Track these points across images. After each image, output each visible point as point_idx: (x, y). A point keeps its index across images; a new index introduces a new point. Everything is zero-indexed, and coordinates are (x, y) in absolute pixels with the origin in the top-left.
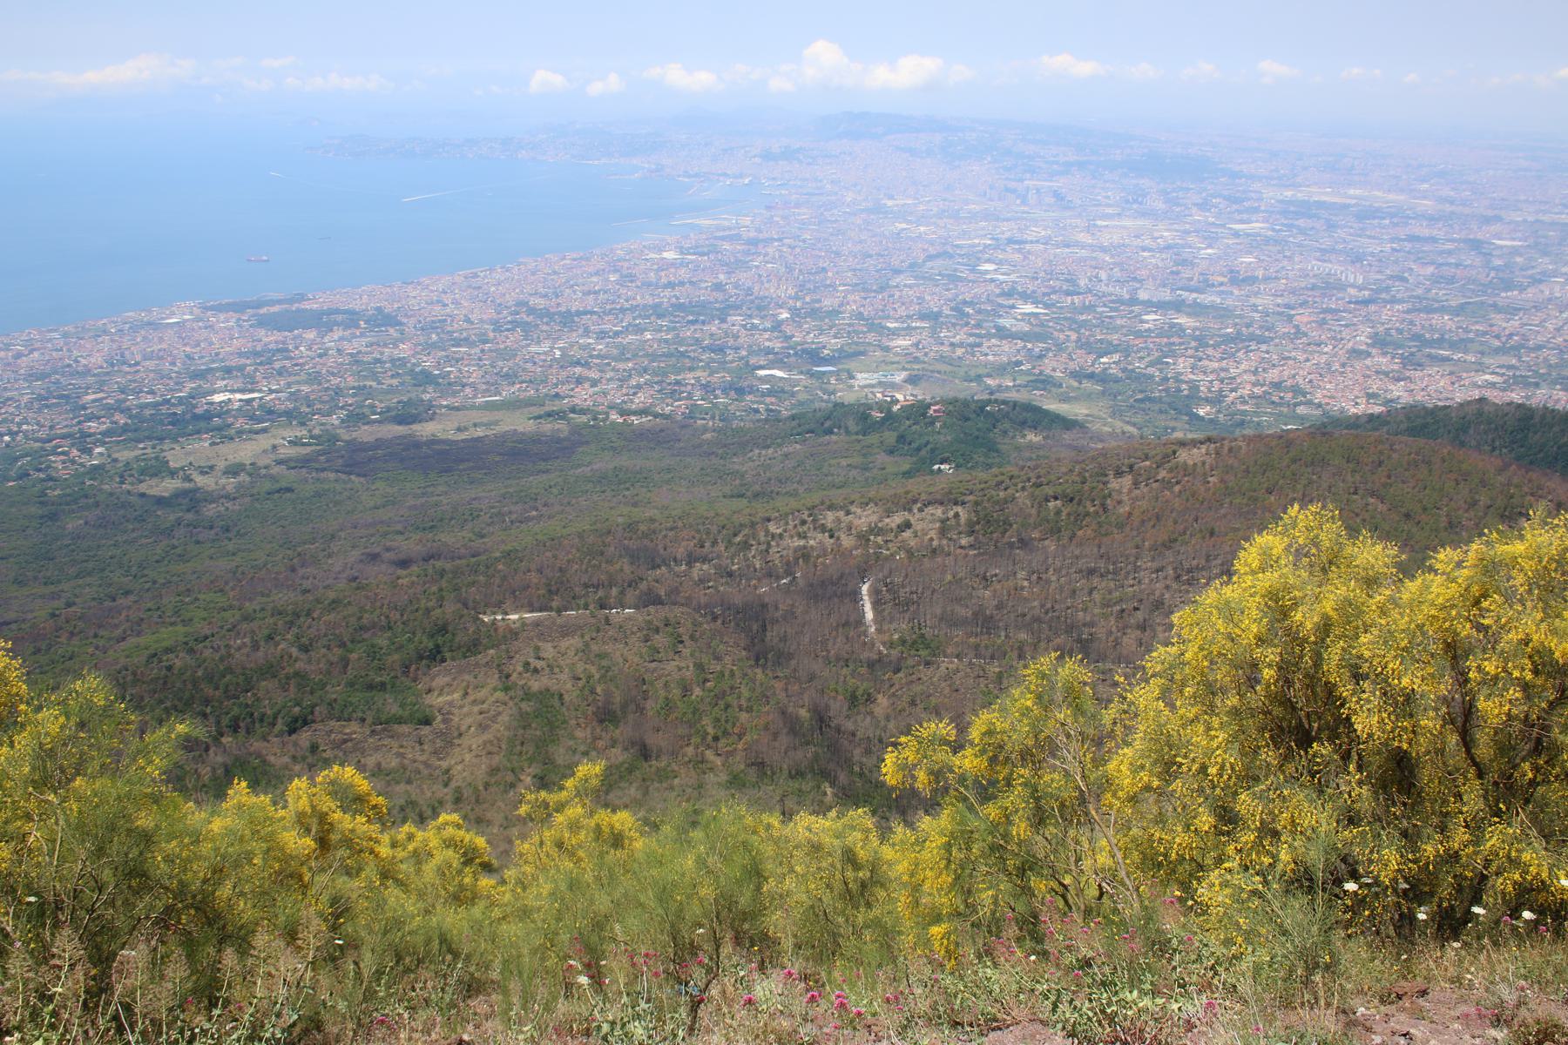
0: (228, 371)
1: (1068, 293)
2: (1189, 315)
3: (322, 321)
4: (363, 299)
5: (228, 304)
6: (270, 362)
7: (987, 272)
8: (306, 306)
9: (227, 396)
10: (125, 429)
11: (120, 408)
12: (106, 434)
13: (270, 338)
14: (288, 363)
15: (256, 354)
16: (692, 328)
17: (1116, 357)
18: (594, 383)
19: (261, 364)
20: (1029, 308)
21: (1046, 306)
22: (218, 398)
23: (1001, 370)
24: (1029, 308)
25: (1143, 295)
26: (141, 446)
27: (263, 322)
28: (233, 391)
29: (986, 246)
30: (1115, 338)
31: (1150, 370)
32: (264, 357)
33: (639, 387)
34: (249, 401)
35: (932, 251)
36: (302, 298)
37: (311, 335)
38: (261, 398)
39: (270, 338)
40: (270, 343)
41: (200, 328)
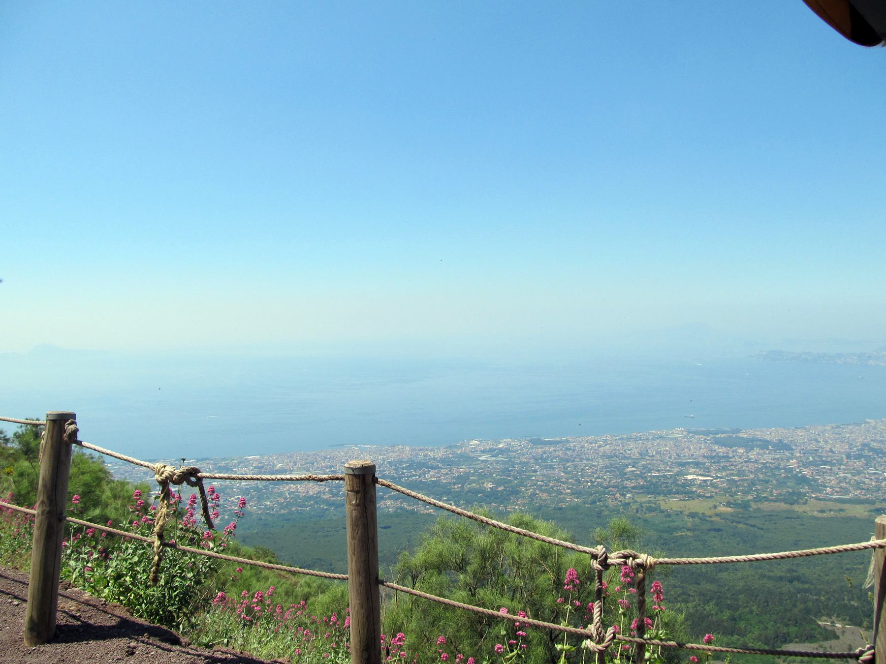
0: (697, 464)
3: (749, 444)
4: (771, 434)
5: (700, 431)
6: (719, 462)
8: (740, 435)
9: (695, 477)
10: (642, 487)
11: (641, 476)
12: (633, 488)
13: (721, 450)
14: (727, 464)
15: (713, 458)
19: (714, 462)
22: (690, 477)
26: (649, 496)
27: (717, 442)
28: (697, 475)
32: (716, 459)
34: (705, 481)
36: (738, 431)
37: (741, 451)
38: (712, 480)
39: (721, 450)
40: (720, 452)
41: (686, 442)
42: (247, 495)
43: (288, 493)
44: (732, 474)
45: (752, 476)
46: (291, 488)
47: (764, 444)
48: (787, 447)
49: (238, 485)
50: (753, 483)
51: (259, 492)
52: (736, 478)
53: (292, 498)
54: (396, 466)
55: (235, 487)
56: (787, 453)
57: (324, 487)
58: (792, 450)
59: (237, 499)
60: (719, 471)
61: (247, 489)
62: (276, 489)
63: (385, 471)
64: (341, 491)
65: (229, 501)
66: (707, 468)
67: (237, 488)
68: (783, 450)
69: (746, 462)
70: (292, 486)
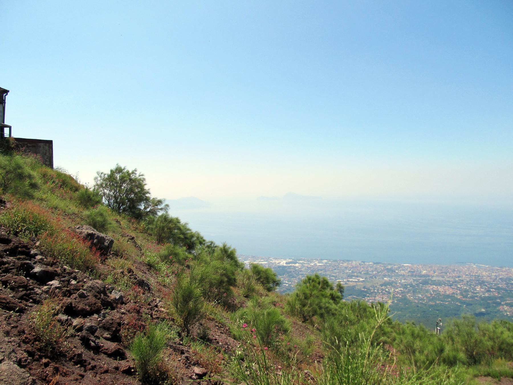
42: (406, 288)
43: (432, 291)
46: (434, 287)
49: (400, 281)
51: (413, 288)
53: (435, 295)
54: (505, 281)
55: (398, 282)
57: (456, 290)
59: (401, 290)
61: (405, 285)
62: (424, 287)
63: (499, 284)
64: (469, 294)
65: (396, 291)
67: (399, 284)
70: (434, 286)
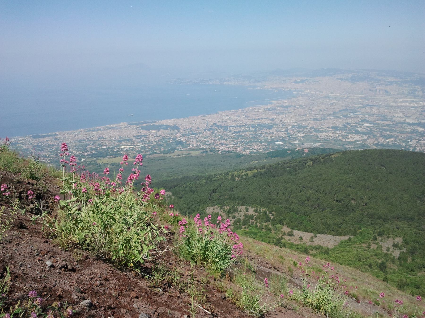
1: (382, 121)
2: (421, 127)
7: (357, 115)
9: (126, 147)
14: (145, 139)
16: (261, 131)
17: (392, 139)
18: (227, 145)
20: (368, 125)
21: (374, 124)
23: (350, 143)
24: (368, 125)
25: (408, 121)
29: (359, 107)
30: (393, 134)
31: (401, 143)
33: (239, 146)
35: (342, 109)
38: (133, 147)
44: (145, 143)
45: (155, 143)
47: (166, 127)
48: (177, 128)
50: (154, 147)
52: (146, 145)
56: (176, 131)
58: (179, 129)
60: (139, 142)
66: (134, 142)
68: (175, 129)
69: (154, 137)
